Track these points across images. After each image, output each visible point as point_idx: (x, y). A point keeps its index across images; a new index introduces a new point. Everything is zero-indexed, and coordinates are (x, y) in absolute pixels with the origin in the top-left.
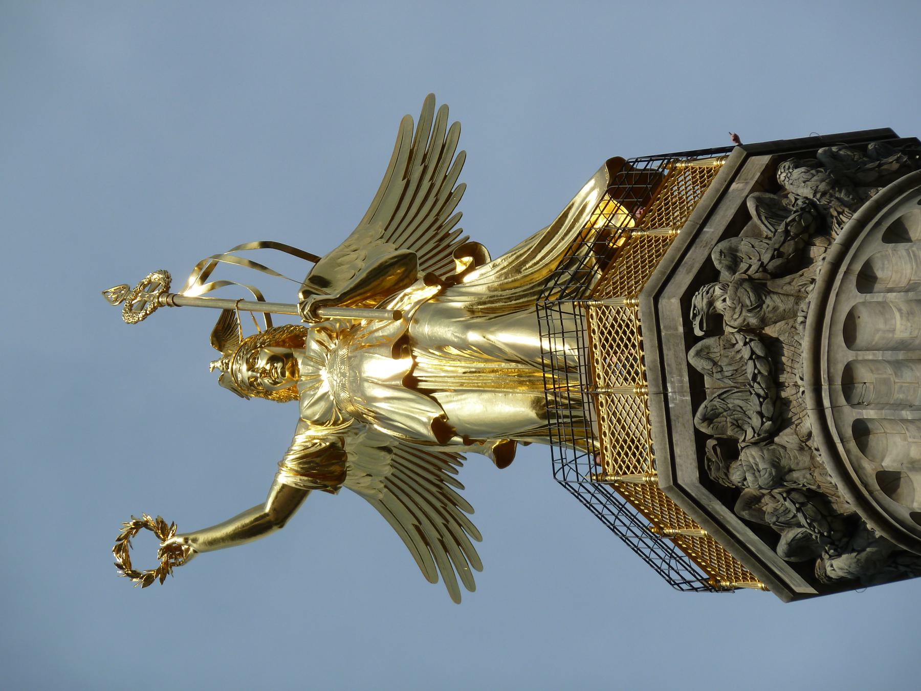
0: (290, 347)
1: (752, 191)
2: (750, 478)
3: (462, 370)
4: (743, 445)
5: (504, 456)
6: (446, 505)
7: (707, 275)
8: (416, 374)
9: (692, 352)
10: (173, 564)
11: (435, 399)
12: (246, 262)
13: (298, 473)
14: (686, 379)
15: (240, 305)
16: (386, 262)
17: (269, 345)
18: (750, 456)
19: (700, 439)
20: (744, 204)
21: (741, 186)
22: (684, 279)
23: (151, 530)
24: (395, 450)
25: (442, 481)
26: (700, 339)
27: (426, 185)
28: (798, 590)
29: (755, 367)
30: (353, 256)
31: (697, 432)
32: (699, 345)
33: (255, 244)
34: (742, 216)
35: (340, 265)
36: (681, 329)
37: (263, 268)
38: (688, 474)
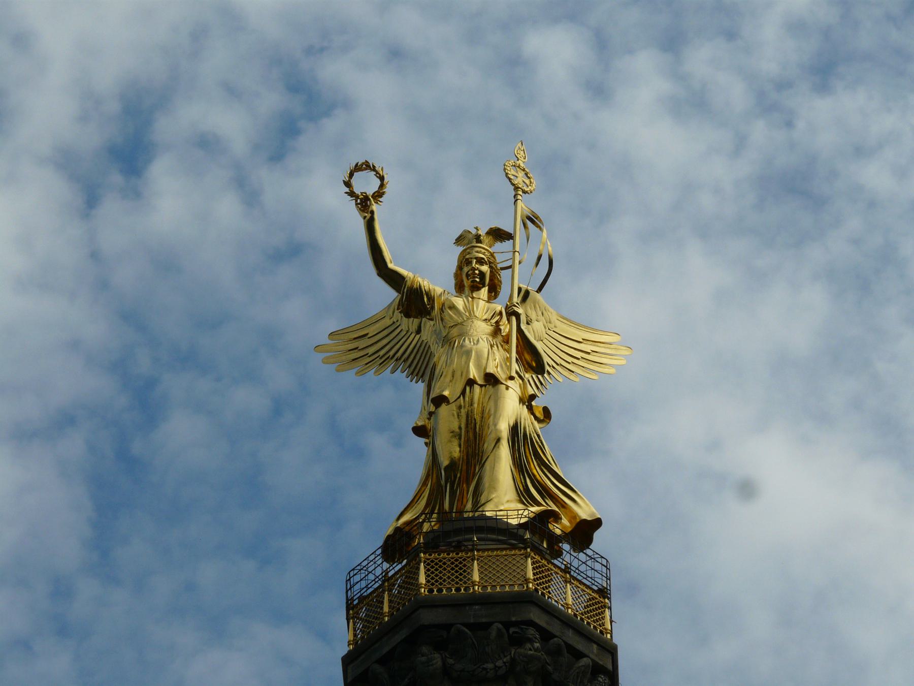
1: (593, 660)
2: (424, 659)
5: (420, 431)
7: (546, 636)
8: (476, 386)
9: (500, 626)
14: (484, 620)
18: (437, 660)
19: (448, 627)
22: (541, 620)
24: (418, 336)
25: (397, 360)
26: (508, 631)
31: (452, 625)
32: (504, 631)
34: (579, 655)
36: (514, 619)
37: (537, 264)
38: (427, 617)
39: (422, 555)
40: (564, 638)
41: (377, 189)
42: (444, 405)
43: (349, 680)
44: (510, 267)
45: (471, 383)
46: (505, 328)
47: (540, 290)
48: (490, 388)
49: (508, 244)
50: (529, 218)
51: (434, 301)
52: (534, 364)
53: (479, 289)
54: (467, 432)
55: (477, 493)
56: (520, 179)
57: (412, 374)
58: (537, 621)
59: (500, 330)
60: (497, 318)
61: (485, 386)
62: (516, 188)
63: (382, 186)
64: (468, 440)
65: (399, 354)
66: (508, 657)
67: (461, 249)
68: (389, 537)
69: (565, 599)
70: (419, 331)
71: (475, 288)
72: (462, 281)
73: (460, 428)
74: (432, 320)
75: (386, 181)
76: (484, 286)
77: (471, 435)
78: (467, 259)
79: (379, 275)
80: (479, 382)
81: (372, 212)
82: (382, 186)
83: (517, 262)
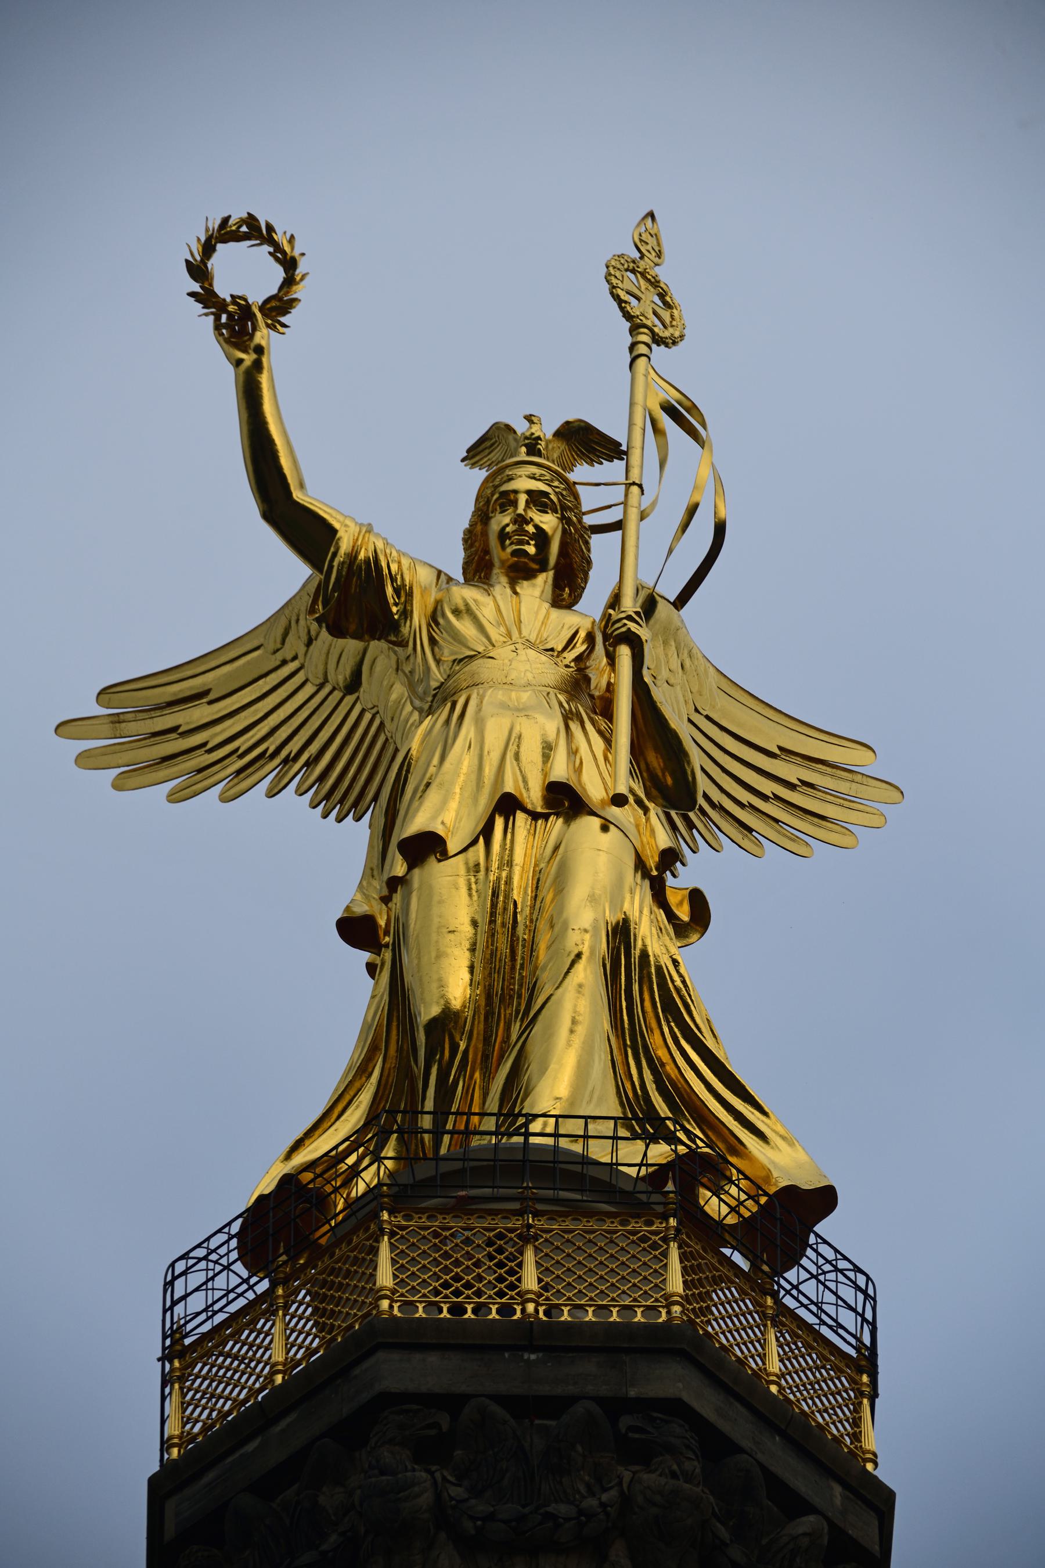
0: (556, 567)
3: (515, 897)
4: (438, 1475)
6: (241, 757)
7: (715, 1445)
8: (520, 816)
10: (218, 318)
11: (474, 842)
12: (696, 498)
13: (352, 556)
15: (635, 489)
16: (689, 762)
17: (564, 531)
19: (451, 1402)
20: (812, 1510)
21: (838, 1501)
22: (706, 1403)
23: (280, 289)
24: (349, 699)
25: (286, 761)
27: (767, 787)
28: (170, 1506)
29: (567, 1520)
30: (675, 664)
31: (465, 1398)
33: (722, 514)
34: (796, 1505)
35: (665, 643)
36: (632, 1393)
39: (385, 1216)
40: (759, 1456)
41: (274, 291)
42: (432, 860)
43: (170, 1530)
44: (618, 526)
45: (508, 805)
46: (599, 677)
47: (682, 600)
48: (557, 824)
49: (613, 470)
50: (669, 409)
51: (410, 595)
52: (669, 781)
53: (529, 575)
54: (492, 934)
55: (516, 1086)
56: (645, 306)
57: (328, 797)
58: (696, 1405)
59: (588, 680)
60: (581, 648)
61: (546, 817)
62: (634, 330)
63: (289, 282)
64: (493, 954)
65: (294, 746)
66: (614, 1493)
67: (480, 475)
68: (262, 1198)
69: (763, 1357)
70: (353, 685)
71: (521, 571)
72: (487, 551)
73: (474, 923)
74: (403, 644)
75: (300, 271)
76: (544, 569)
77: (502, 944)
78: (505, 494)
79: (268, 516)
80: (529, 807)
81: (259, 350)
82: (289, 282)
83: (633, 514)
